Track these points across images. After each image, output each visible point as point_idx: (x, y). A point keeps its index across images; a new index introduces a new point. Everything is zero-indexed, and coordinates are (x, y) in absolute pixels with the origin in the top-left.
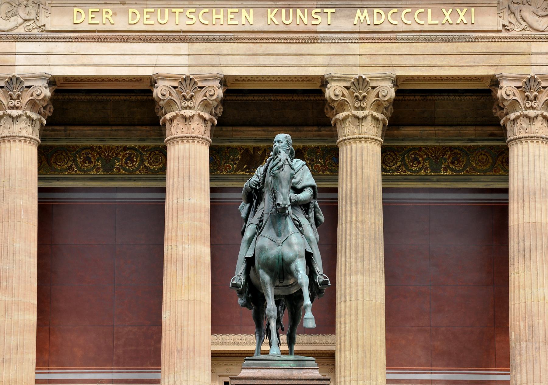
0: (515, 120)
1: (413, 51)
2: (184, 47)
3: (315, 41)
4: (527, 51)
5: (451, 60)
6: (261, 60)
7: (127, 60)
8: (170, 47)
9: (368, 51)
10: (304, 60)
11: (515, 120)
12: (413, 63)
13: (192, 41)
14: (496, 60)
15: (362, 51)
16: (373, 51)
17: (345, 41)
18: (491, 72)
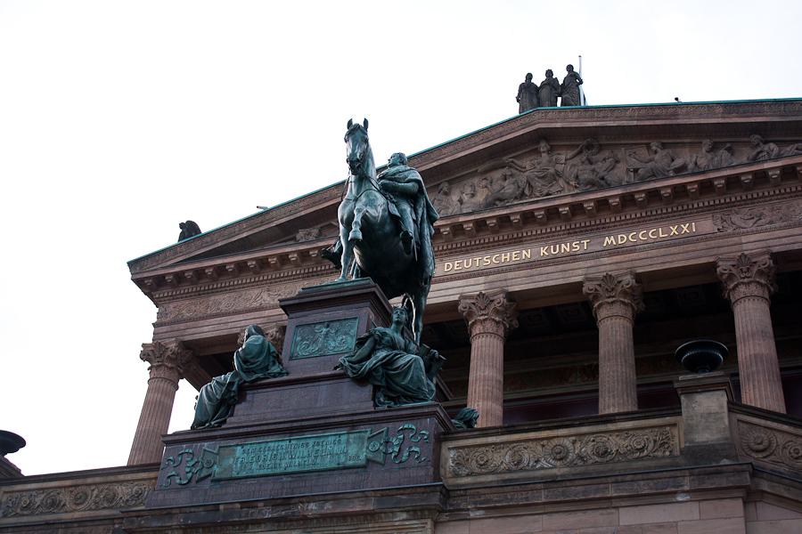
0: (734, 288)
1: (649, 255)
2: (482, 279)
3: (575, 260)
4: (739, 242)
5: (679, 257)
6: (537, 278)
7: (443, 293)
8: (472, 281)
9: (615, 261)
10: (567, 274)
11: (734, 288)
12: (650, 263)
13: (487, 274)
14: (715, 251)
15: (610, 262)
16: (619, 261)
17: (598, 258)
18: (711, 260)
